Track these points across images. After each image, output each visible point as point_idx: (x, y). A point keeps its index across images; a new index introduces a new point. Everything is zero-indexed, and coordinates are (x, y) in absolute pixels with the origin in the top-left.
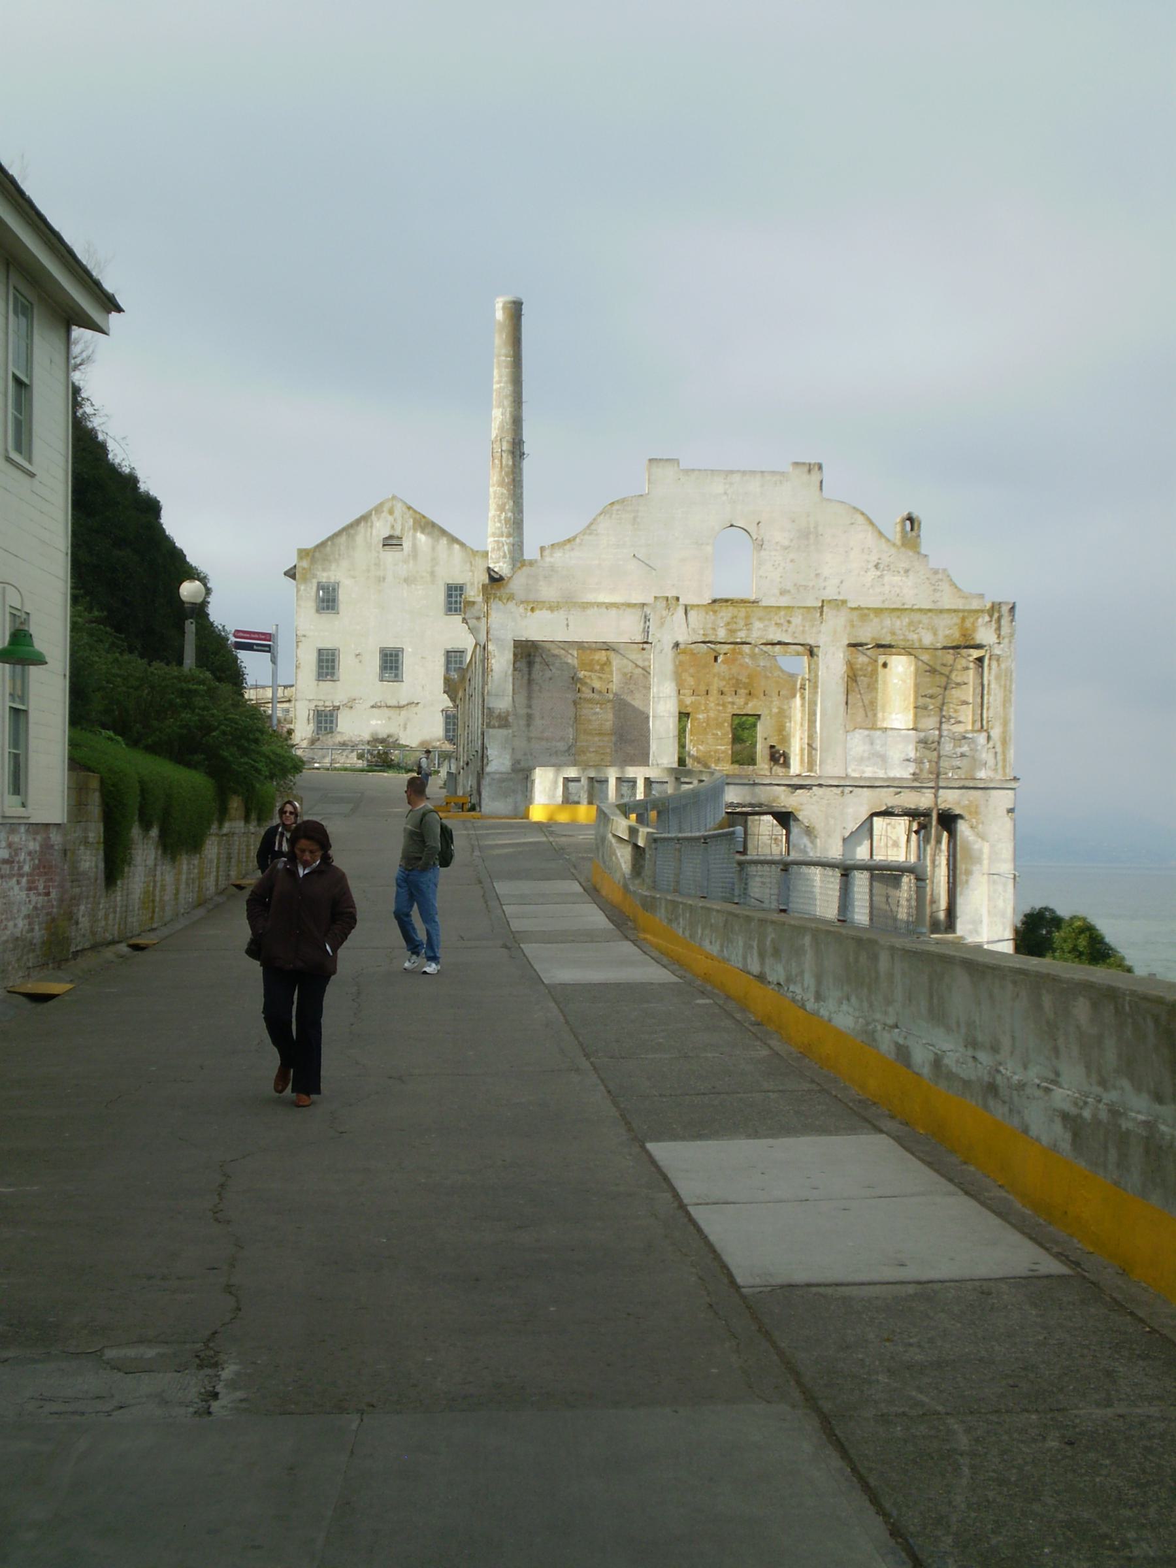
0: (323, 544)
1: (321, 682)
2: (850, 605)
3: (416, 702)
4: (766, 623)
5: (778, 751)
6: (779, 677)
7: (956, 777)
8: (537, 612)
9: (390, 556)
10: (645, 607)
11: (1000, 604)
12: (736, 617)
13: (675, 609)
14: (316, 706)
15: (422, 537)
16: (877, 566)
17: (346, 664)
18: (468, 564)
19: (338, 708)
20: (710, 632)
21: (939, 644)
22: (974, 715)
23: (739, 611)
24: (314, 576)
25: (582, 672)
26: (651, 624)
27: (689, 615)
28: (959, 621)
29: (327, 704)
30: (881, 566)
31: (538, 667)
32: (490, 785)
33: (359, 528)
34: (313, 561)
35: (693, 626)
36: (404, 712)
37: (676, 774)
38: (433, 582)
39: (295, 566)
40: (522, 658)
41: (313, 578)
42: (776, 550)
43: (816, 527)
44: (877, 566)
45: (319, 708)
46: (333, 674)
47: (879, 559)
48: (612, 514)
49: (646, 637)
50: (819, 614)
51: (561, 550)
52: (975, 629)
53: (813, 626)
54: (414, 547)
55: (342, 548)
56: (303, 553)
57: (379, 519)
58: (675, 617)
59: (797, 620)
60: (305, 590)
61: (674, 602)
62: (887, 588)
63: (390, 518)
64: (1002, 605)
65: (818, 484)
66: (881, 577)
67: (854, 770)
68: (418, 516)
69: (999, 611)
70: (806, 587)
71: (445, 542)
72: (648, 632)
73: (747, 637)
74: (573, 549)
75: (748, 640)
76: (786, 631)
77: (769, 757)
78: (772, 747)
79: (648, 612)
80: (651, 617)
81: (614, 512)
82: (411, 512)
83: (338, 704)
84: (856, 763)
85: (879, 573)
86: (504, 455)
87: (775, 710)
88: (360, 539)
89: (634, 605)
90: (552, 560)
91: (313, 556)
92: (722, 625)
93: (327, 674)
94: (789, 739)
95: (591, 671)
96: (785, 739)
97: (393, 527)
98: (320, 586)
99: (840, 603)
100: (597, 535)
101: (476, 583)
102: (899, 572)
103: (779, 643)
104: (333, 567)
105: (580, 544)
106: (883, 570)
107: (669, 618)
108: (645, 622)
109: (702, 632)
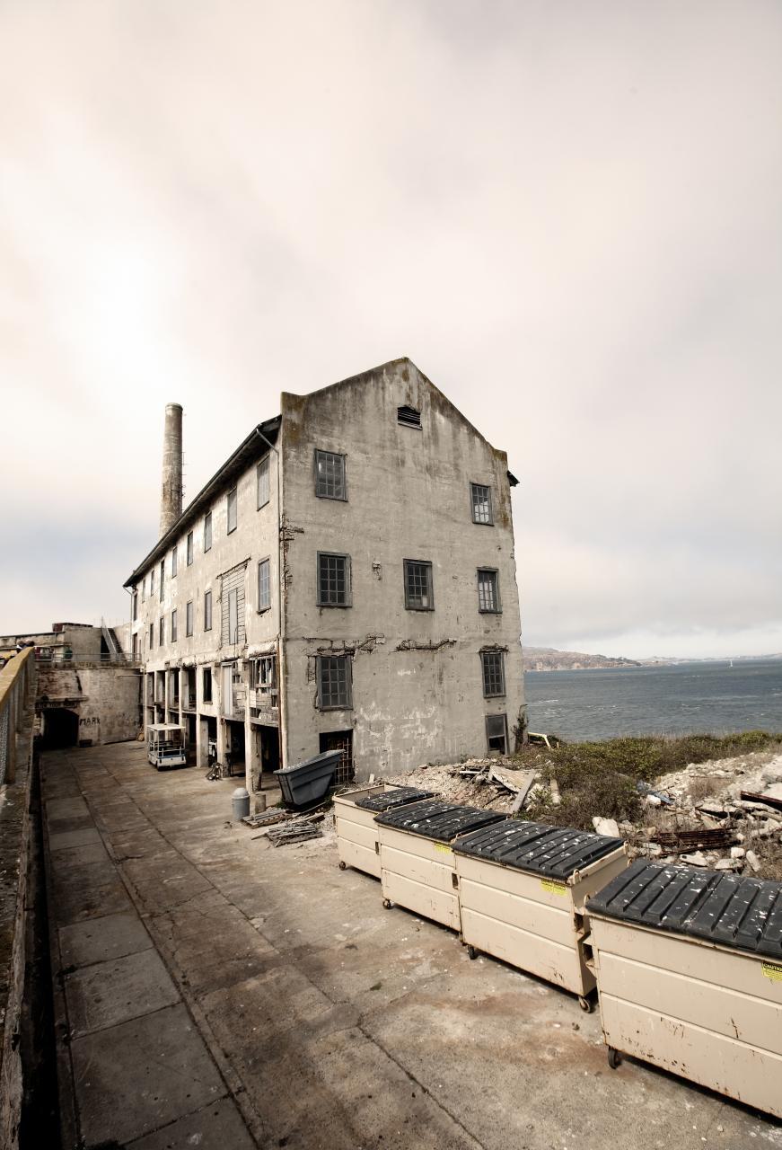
0: (319, 396)
1: (325, 610)
3: (451, 640)
9: (406, 434)
14: (318, 650)
15: (441, 419)
17: (359, 579)
18: (490, 464)
19: (351, 652)
24: (310, 439)
29: (338, 645)
33: (368, 386)
34: (307, 416)
36: (438, 656)
38: (458, 477)
41: (308, 441)
45: (325, 653)
54: (434, 427)
55: (348, 408)
57: (391, 382)
63: (404, 384)
68: (435, 392)
71: (466, 431)
82: (427, 384)
83: (352, 646)
86: (173, 493)
88: (369, 399)
91: (307, 410)
97: (408, 396)
101: (499, 488)
104: (336, 431)
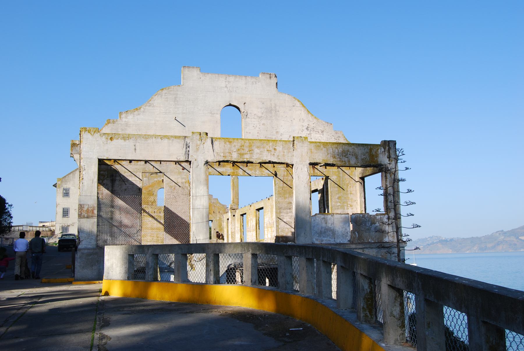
2: (309, 140)
4: (262, 150)
5: (219, 234)
6: (219, 206)
7: (373, 242)
8: (115, 141)
10: (186, 138)
11: (389, 141)
12: (243, 146)
13: (205, 140)
16: (307, 129)
19: (69, 226)
20: (228, 155)
21: (359, 164)
22: (361, 207)
23: (245, 142)
25: (145, 205)
26: (190, 149)
27: (214, 146)
28: (368, 151)
31: (118, 183)
32: (80, 258)
33: (76, 172)
35: (217, 151)
37: (252, 250)
39: (56, 183)
40: (108, 177)
41: (62, 187)
42: (255, 118)
43: (275, 107)
44: (307, 129)
46: (68, 215)
48: (162, 95)
49: (187, 157)
50: (292, 145)
51: (132, 115)
52: (377, 156)
53: (289, 152)
56: (59, 179)
58: (205, 145)
59: (279, 148)
60: (59, 190)
61: (205, 135)
64: (390, 142)
65: (276, 85)
67: (317, 240)
69: (389, 145)
72: (188, 155)
73: (250, 158)
74: (139, 114)
75: (251, 160)
76: (274, 155)
77: (216, 236)
78: (217, 232)
79: (188, 142)
80: (190, 145)
81: (164, 94)
83: (69, 225)
84: (318, 235)
85: (308, 132)
87: (218, 218)
89: (179, 137)
90: (127, 120)
91: (62, 180)
92: (235, 151)
93: (66, 216)
94: (224, 229)
95: (148, 205)
96: (222, 229)
98: (64, 189)
99: (304, 139)
100: (154, 106)
102: (319, 132)
103: (270, 162)
105: (144, 112)
106: (311, 131)
107: (202, 146)
108: (186, 148)
109: (222, 155)
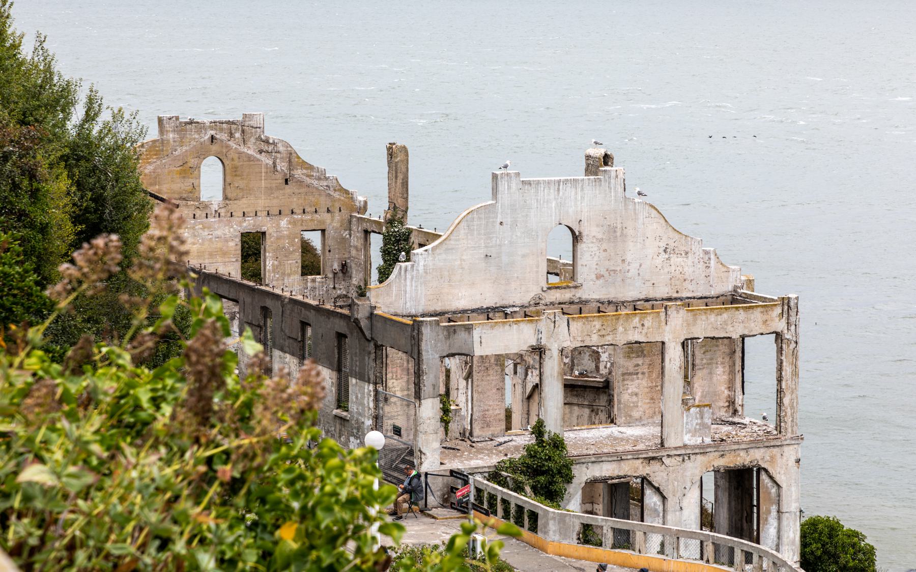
30: (668, 250)
42: (593, 243)
44: (665, 251)
47: (667, 245)
62: (673, 268)
66: (669, 259)
70: (615, 271)
